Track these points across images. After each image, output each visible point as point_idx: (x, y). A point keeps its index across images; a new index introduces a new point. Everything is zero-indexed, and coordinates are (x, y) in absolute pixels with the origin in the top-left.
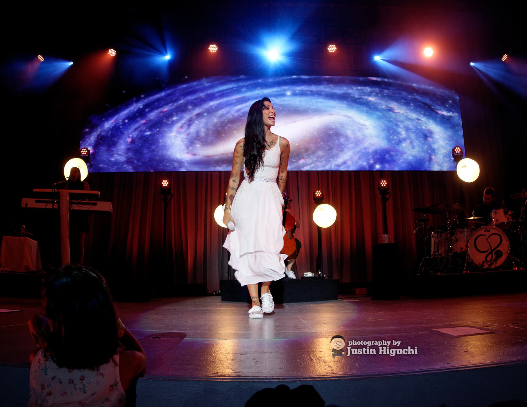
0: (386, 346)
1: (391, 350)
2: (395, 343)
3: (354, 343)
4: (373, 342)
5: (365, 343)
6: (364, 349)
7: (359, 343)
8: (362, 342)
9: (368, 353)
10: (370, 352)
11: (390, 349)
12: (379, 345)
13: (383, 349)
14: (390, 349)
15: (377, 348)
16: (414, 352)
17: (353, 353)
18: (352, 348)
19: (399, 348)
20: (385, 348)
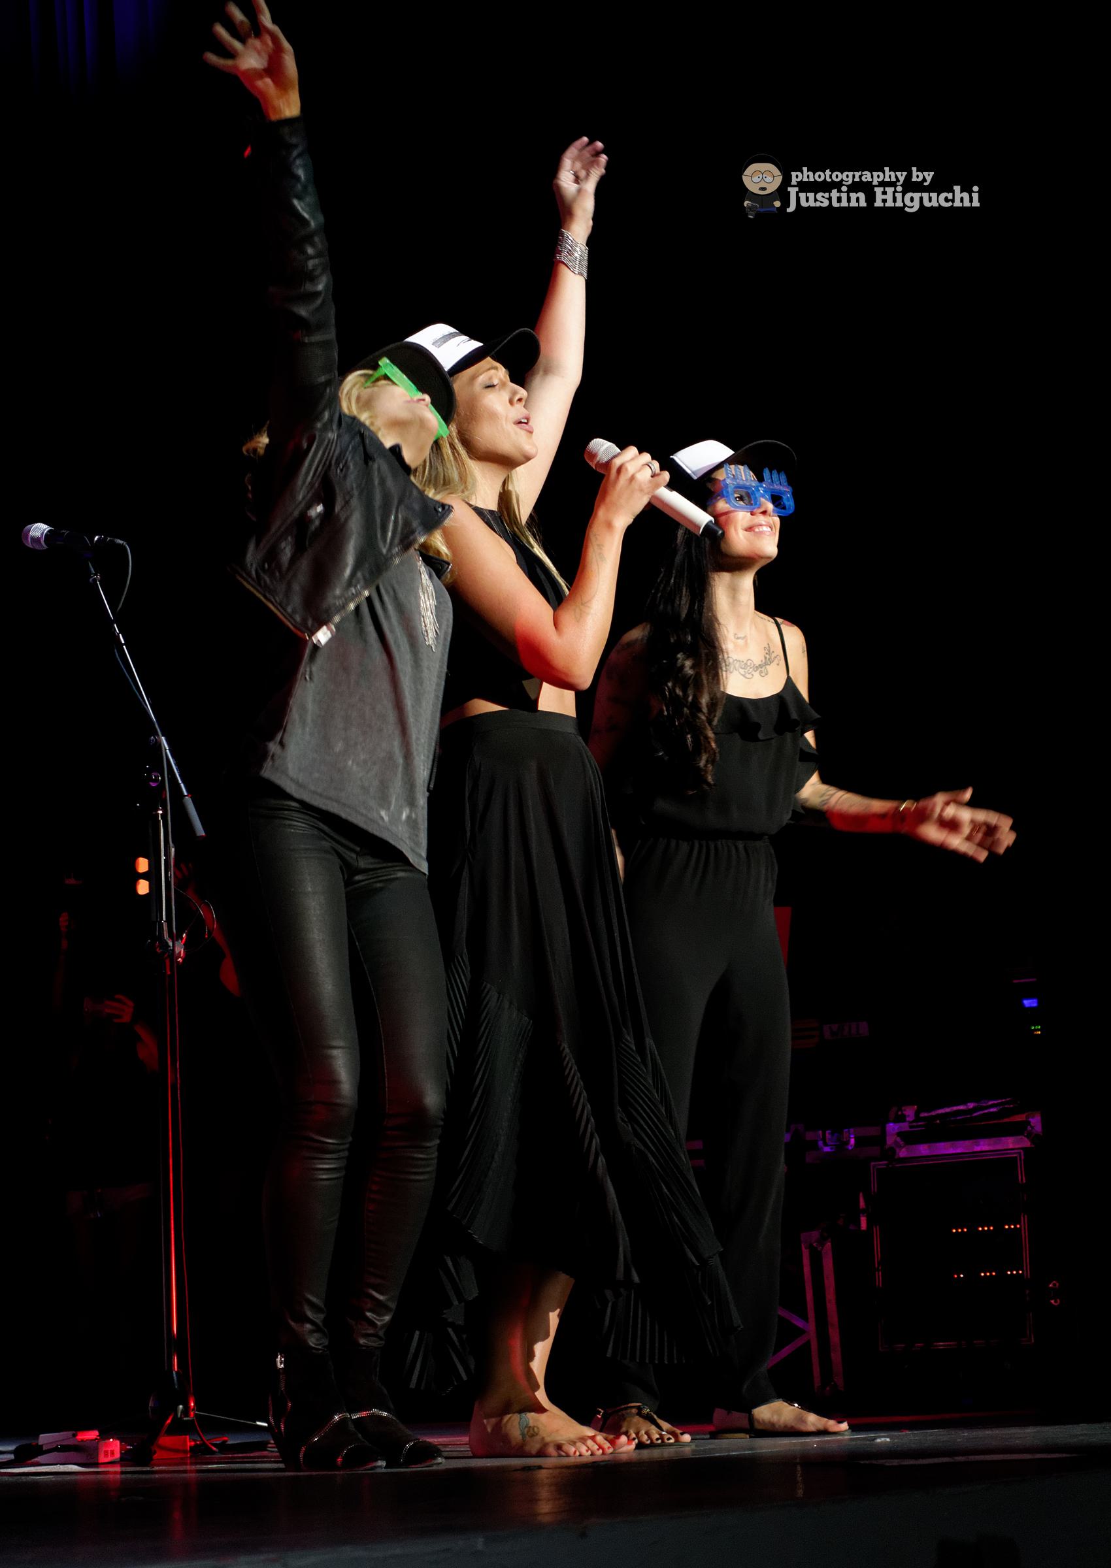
0: (893, 184)
2: (917, 176)
3: (806, 175)
4: (857, 174)
5: (837, 176)
6: (835, 194)
7: (820, 176)
8: (828, 172)
9: (844, 204)
10: (849, 200)
12: (875, 183)
13: (884, 193)
16: (971, 200)
18: (800, 191)
19: (928, 189)
20: (890, 190)
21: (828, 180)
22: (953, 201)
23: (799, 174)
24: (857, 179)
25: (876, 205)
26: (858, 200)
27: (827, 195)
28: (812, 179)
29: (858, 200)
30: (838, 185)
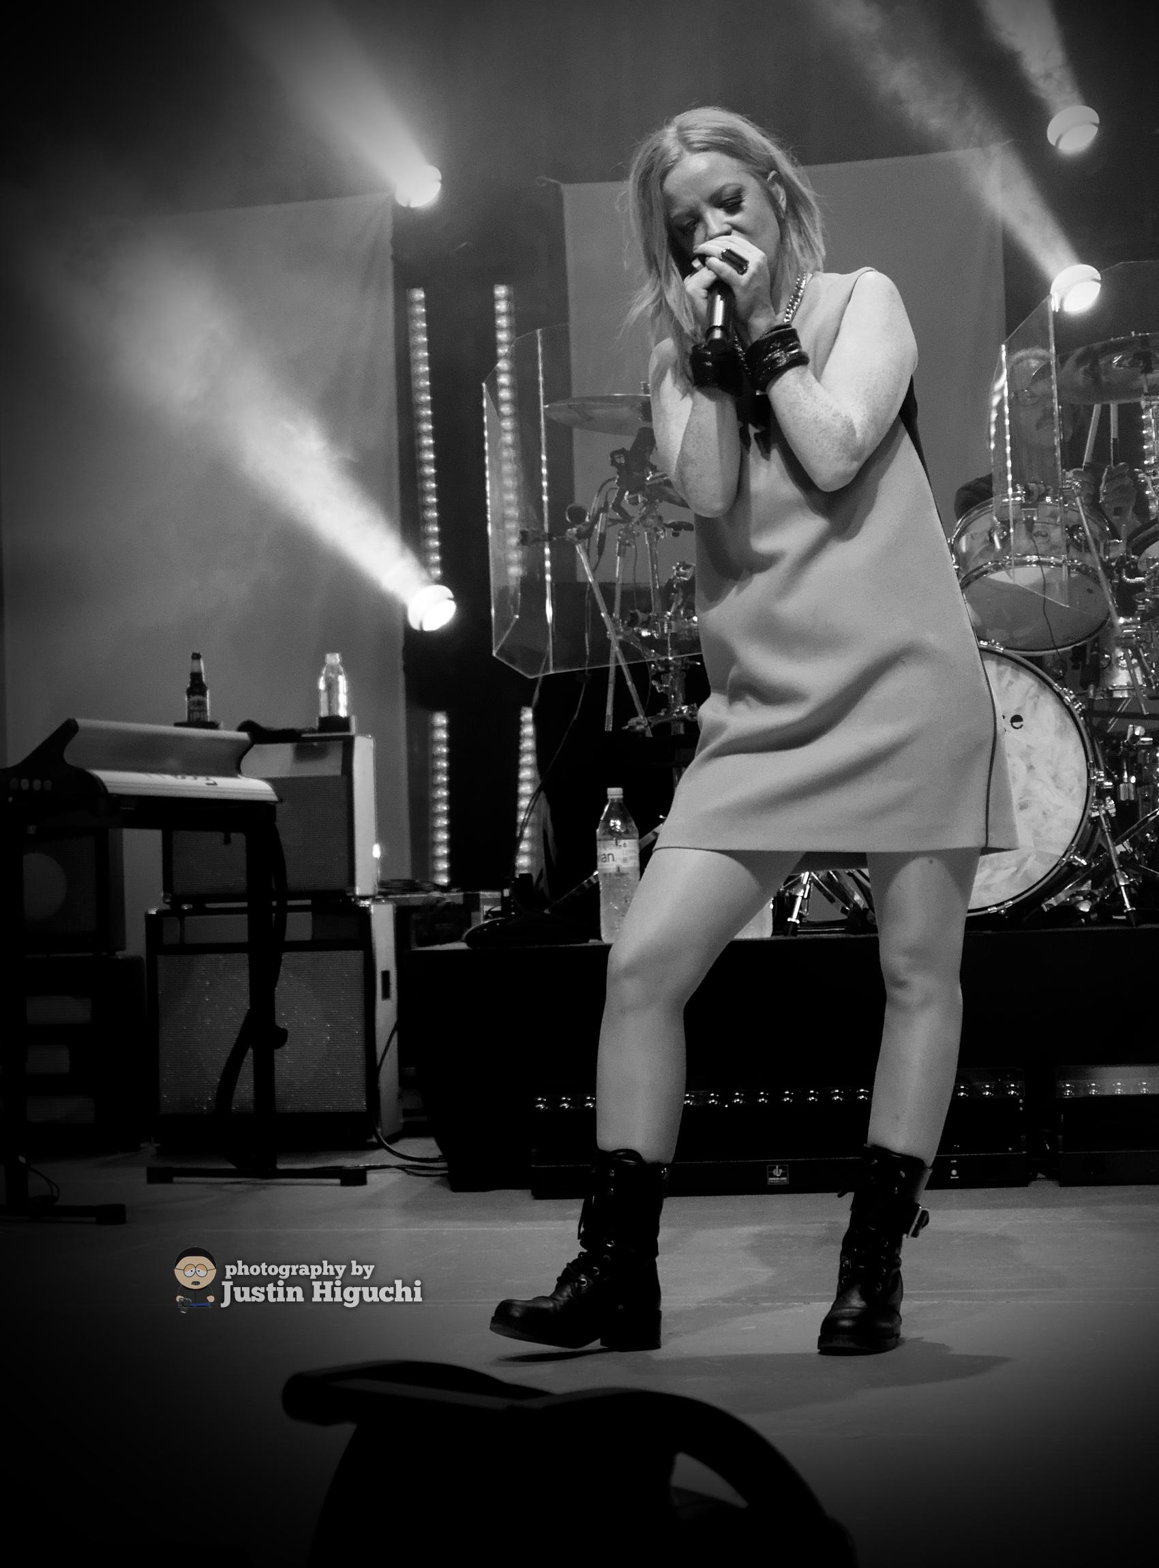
0: (329, 1278)
1: (347, 1290)
2: (356, 1270)
3: (241, 1269)
4: (294, 1268)
5: (274, 1270)
7: (255, 1270)
8: (264, 1266)
9: (281, 1298)
10: (286, 1295)
11: (343, 1288)
12: (313, 1277)
13: (323, 1287)
14: (343, 1288)
15: (305, 1283)
16: (413, 1295)
17: (238, 1298)
19: (369, 1284)
20: (328, 1284)
21: (264, 1273)
22: (394, 1295)
23: (234, 1267)
24: (294, 1273)
25: (314, 1300)
27: (262, 1290)
28: (247, 1273)
30: (274, 1279)
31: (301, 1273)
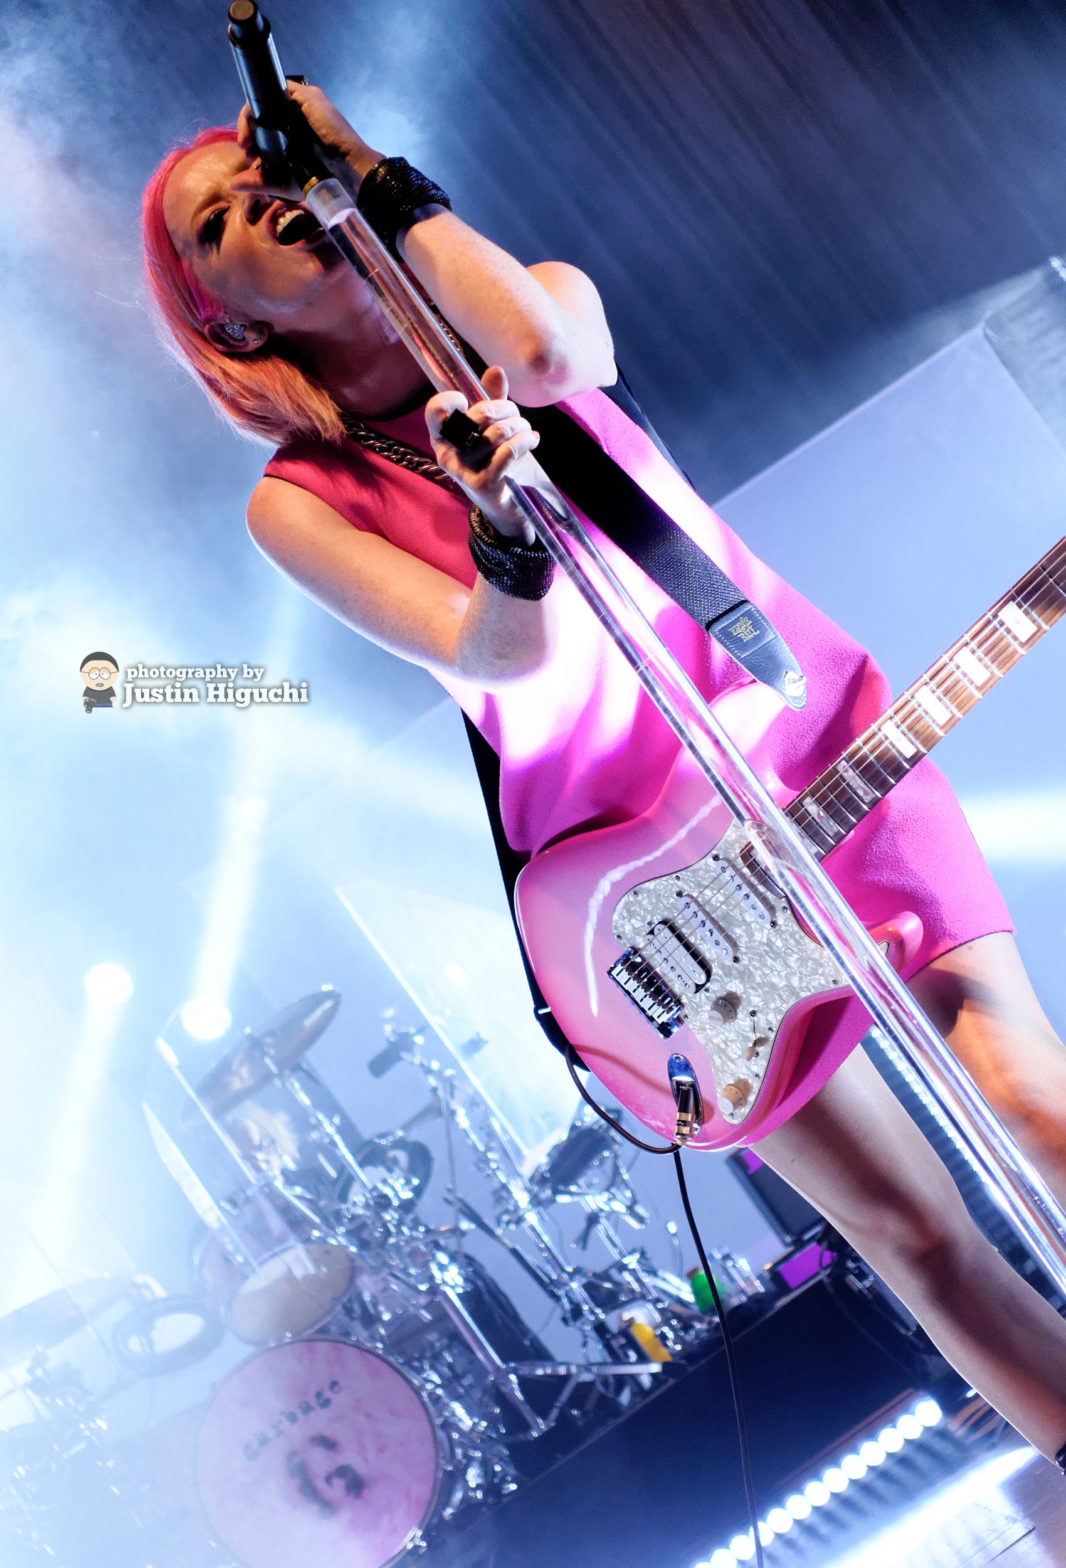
0: (222, 680)
10: (182, 696)
12: (208, 679)
13: (216, 689)
16: (300, 696)
22: (282, 696)
24: (190, 675)
26: (191, 695)
29: (191, 695)
31: (196, 675)
